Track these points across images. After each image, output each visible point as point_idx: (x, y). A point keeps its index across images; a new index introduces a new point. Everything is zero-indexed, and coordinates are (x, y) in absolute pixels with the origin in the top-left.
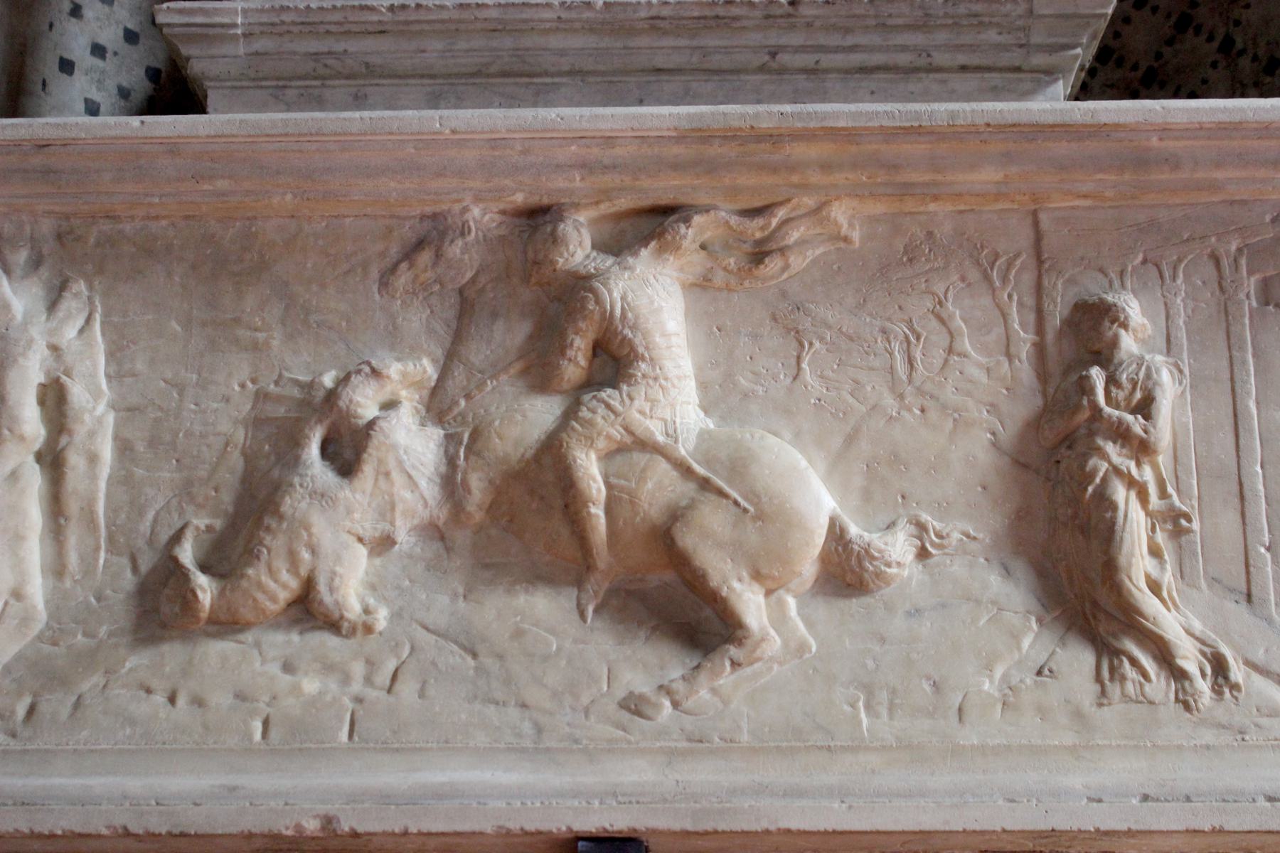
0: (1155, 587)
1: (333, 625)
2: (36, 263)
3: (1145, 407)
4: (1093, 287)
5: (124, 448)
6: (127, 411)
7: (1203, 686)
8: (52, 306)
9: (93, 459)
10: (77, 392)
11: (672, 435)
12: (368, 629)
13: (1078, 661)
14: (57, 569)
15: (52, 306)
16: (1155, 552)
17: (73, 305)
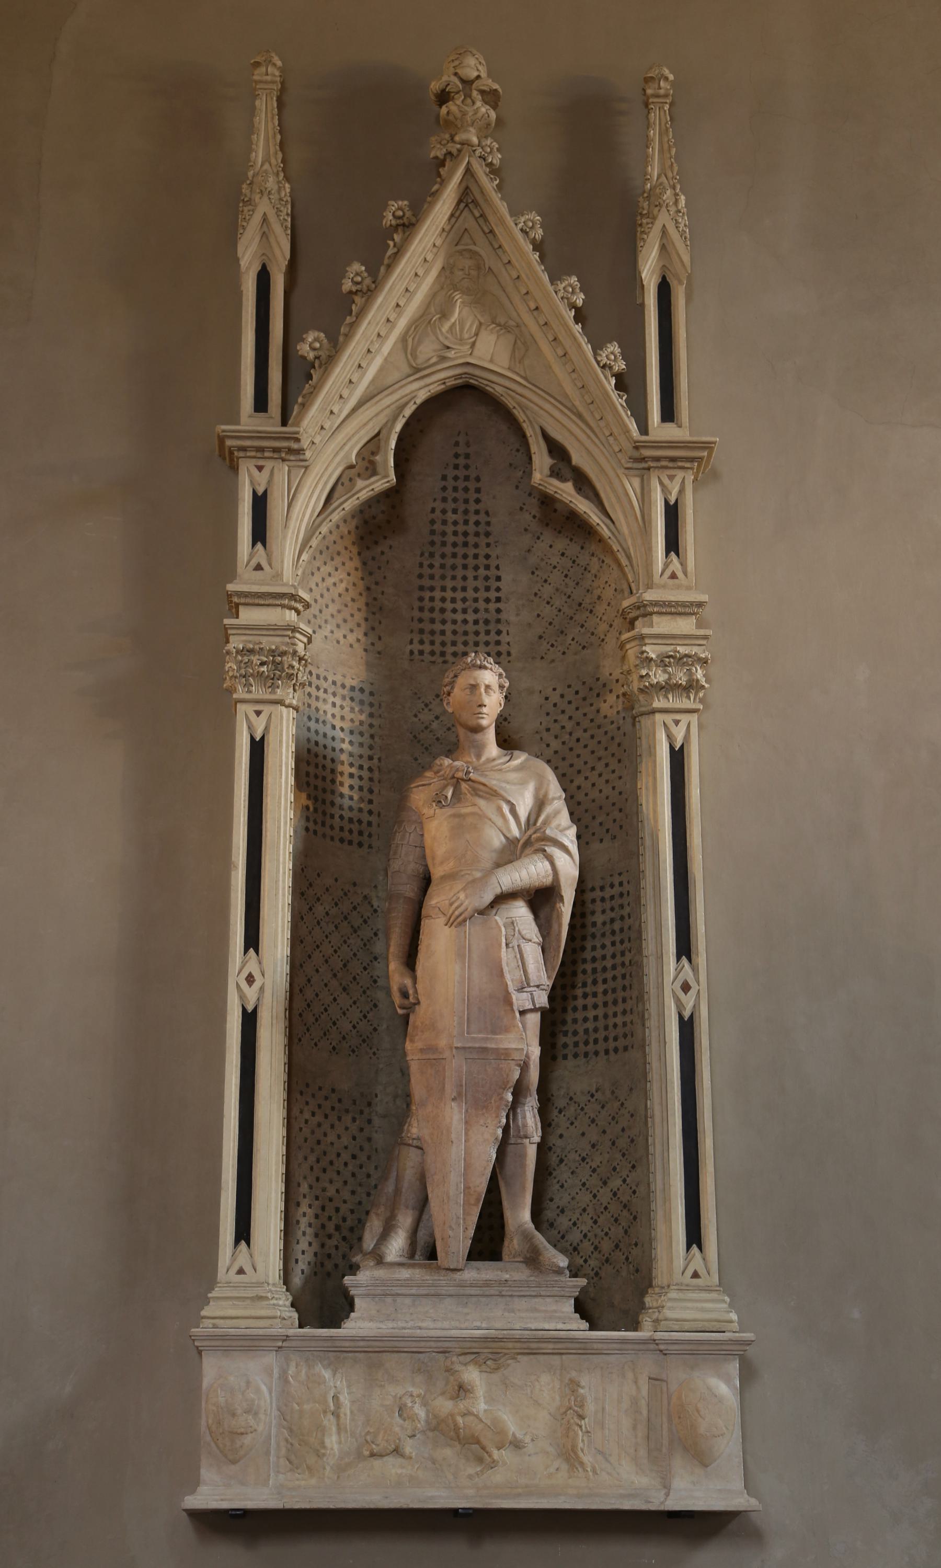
0: (582, 1450)
1: (402, 1456)
2: (329, 1365)
3: (582, 1406)
4: (574, 1374)
5: (352, 1412)
6: (353, 1402)
7: (591, 1474)
8: (334, 1375)
9: (345, 1415)
10: (341, 1398)
11: (478, 1412)
12: (411, 1458)
13: (565, 1467)
14: (340, 1443)
15: (334, 1375)
16: (583, 1441)
17: (338, 1375)
